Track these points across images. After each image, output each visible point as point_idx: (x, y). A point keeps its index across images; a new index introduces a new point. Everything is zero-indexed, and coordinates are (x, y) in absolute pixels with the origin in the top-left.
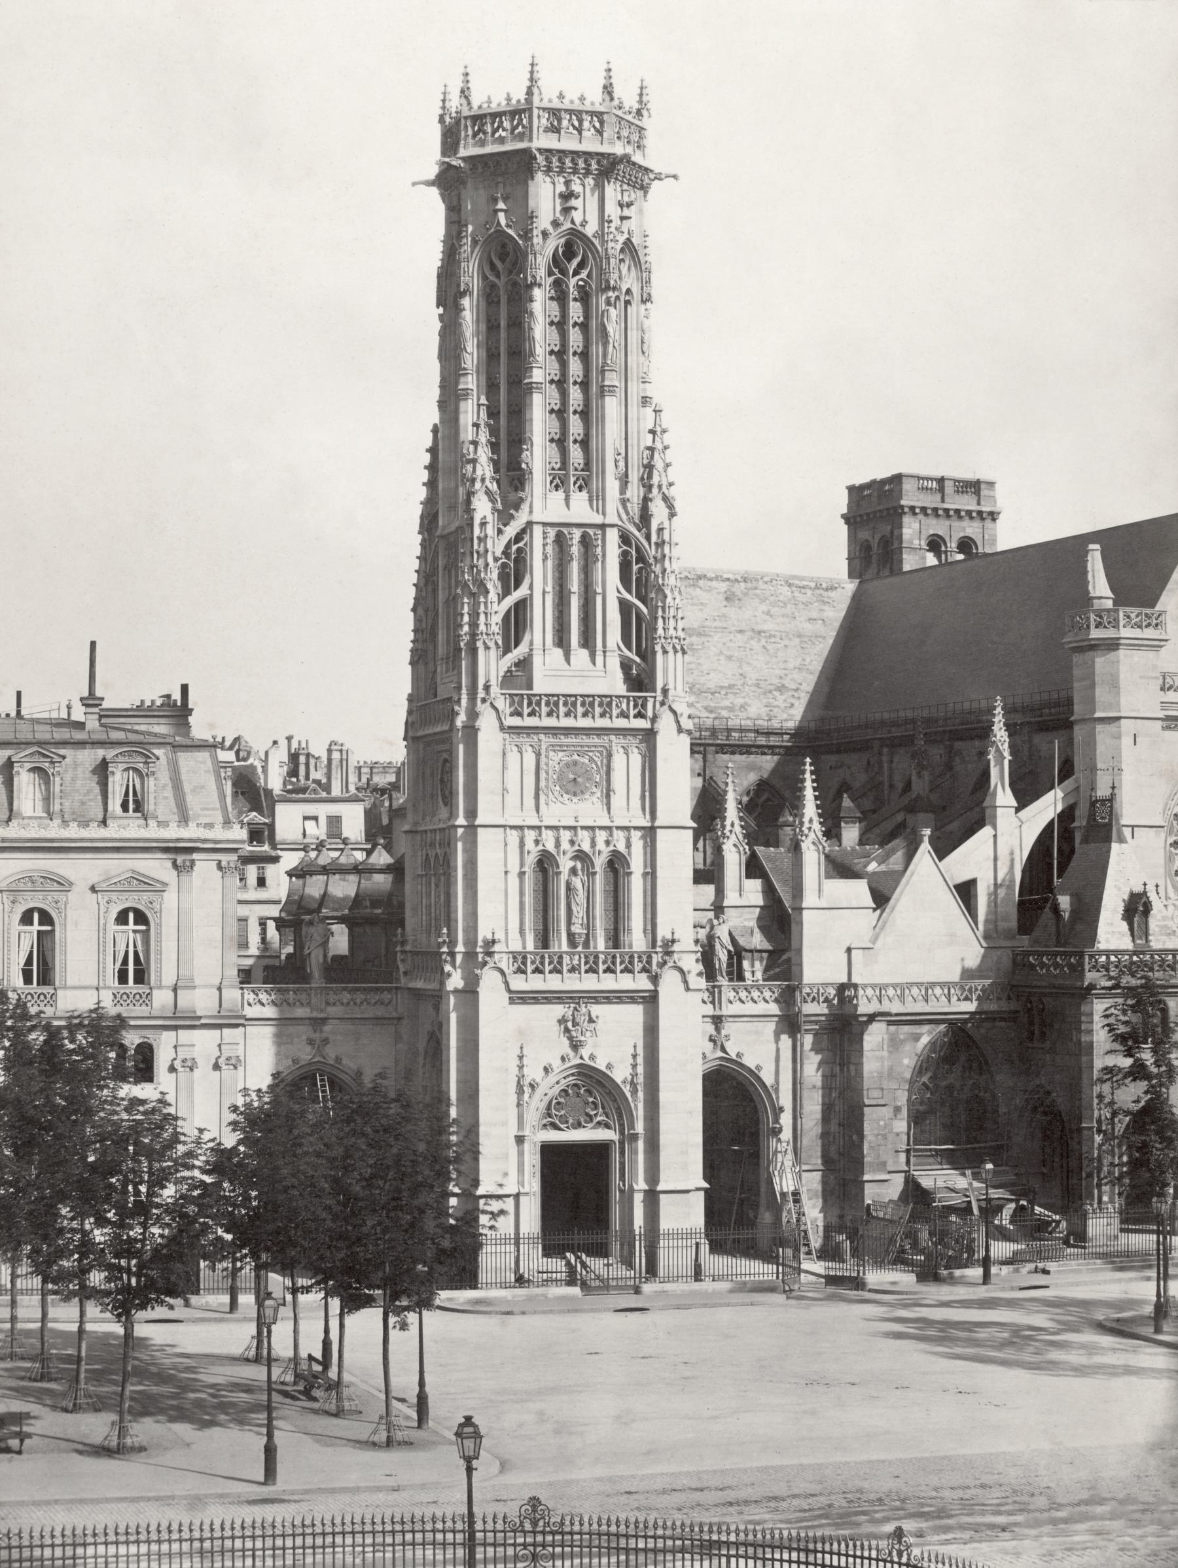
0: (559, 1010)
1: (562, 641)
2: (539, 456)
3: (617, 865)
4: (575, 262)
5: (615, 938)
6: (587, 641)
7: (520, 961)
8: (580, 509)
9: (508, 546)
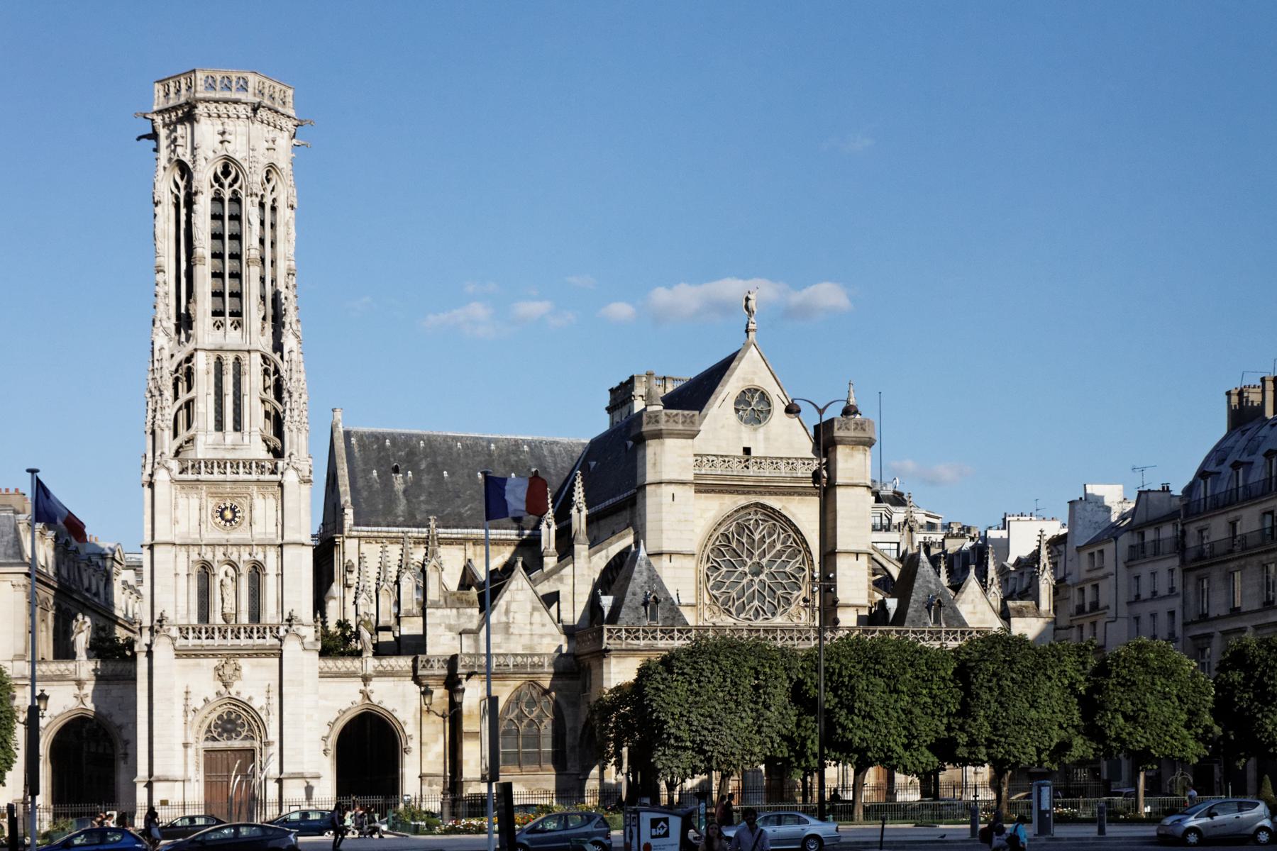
0: (215, 662)
1: (220, 426)
2: (204, 304)
4: (230, 179)
6: (238, 426)
7: (184, 631)
8: (232, 338)
9: (180, 365)
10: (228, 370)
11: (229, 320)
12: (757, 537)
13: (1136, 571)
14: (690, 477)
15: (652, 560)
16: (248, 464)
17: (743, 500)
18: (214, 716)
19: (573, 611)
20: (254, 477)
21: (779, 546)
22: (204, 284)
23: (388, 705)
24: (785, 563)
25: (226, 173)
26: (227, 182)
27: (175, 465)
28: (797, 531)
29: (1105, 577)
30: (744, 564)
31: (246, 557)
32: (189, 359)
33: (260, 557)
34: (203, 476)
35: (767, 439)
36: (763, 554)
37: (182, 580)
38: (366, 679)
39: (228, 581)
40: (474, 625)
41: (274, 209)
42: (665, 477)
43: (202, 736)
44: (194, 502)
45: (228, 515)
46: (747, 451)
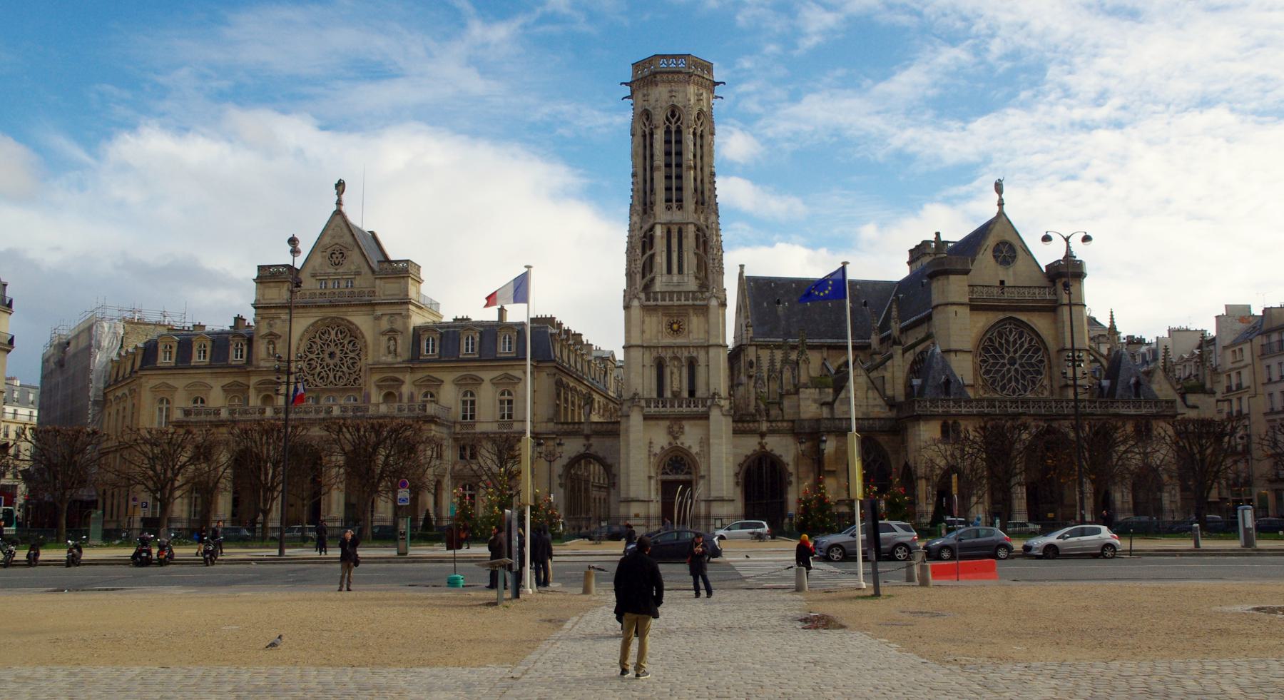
0: (667, 423)
1: (669, 271)
3: (692, 364)
5: (692, 393)
6: (680, 271)
7: (648, 402)
8: (677, 216)
10: (675, 233)
11: (674, 205)
12: (1011, 339)
13: (1268, 362)
14: (966, 300)
15: (946, 356)
16: (687, 293)
17: (1001, 316)
18: (667, 459)
19: (897, 389)
20: (690, 302)
21: (1026, 346)
22: (660, 183)
23: (777, 452)
24: (1031, 357)
25: (673, 115)
27: (642, 296)
29: (1246, 366)
30: (1003, 357)
31: (686, 354)
32: (652, 228)
33: (695, 354)
34: (660, 303)
35: (1015, 274)
36: (1015, 352)
37: (647, 371)
38: (762, 435)
39: (675, 370)
40: (830, 399)
41: (702, 136)
42: (951, 300)
43: (660, 471)
44: (654, 319)
45: (675, 327)
46: (1002, 282)
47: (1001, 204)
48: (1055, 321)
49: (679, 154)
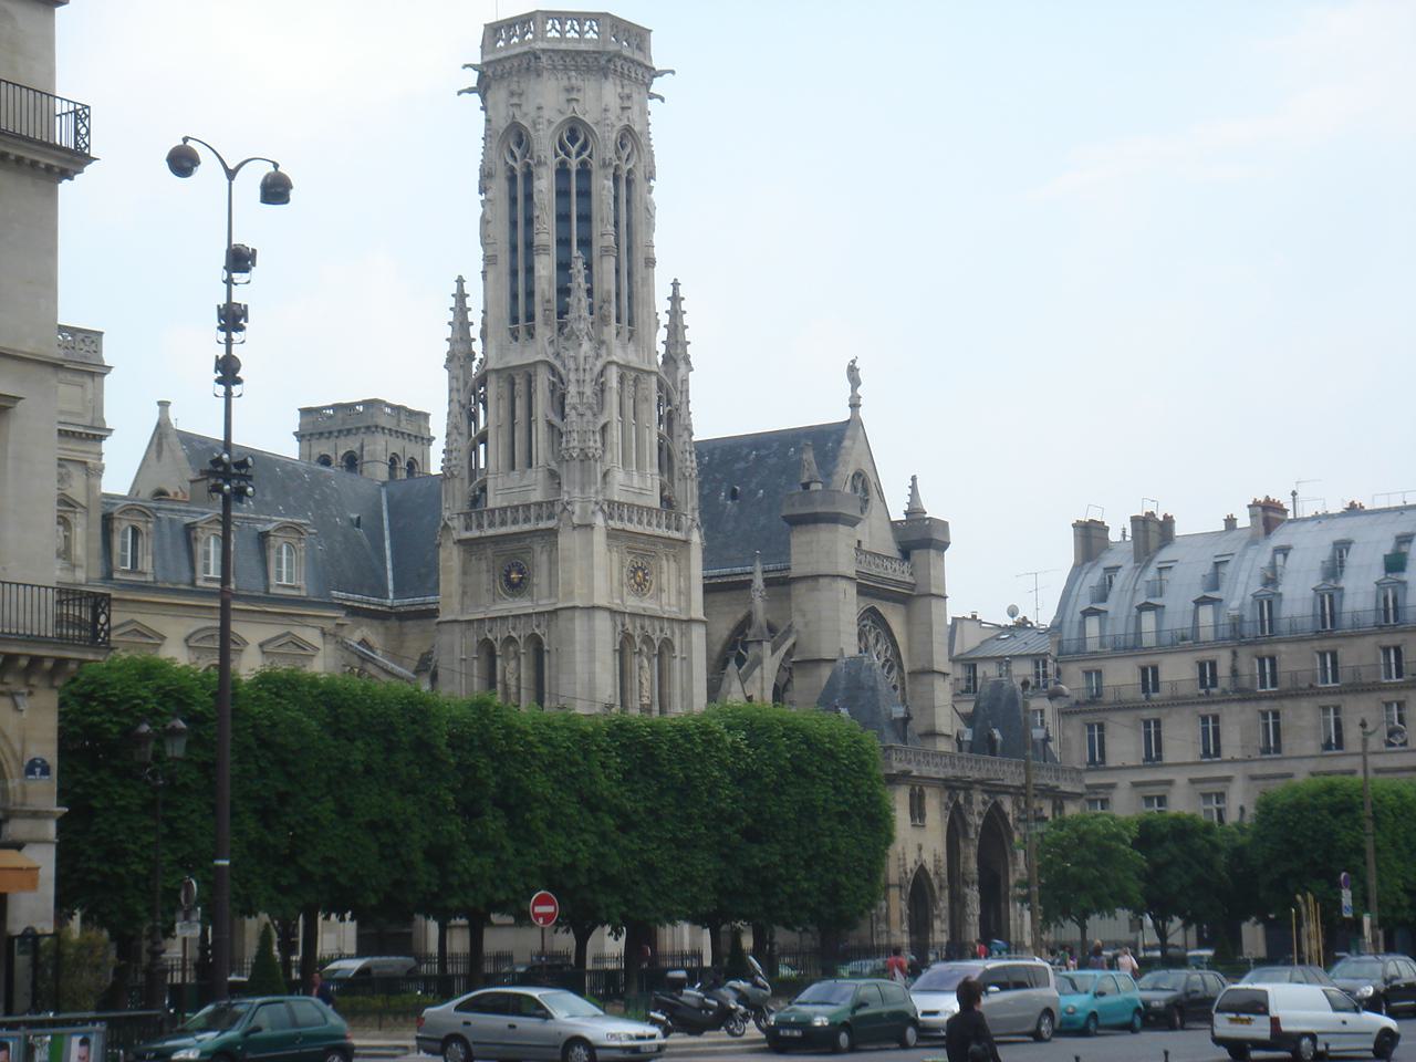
25: (573, 139)
26: (574, 150)
28: (894, 643)
47: (855, 405)
48: (909, 621)
49: (586, 218)
